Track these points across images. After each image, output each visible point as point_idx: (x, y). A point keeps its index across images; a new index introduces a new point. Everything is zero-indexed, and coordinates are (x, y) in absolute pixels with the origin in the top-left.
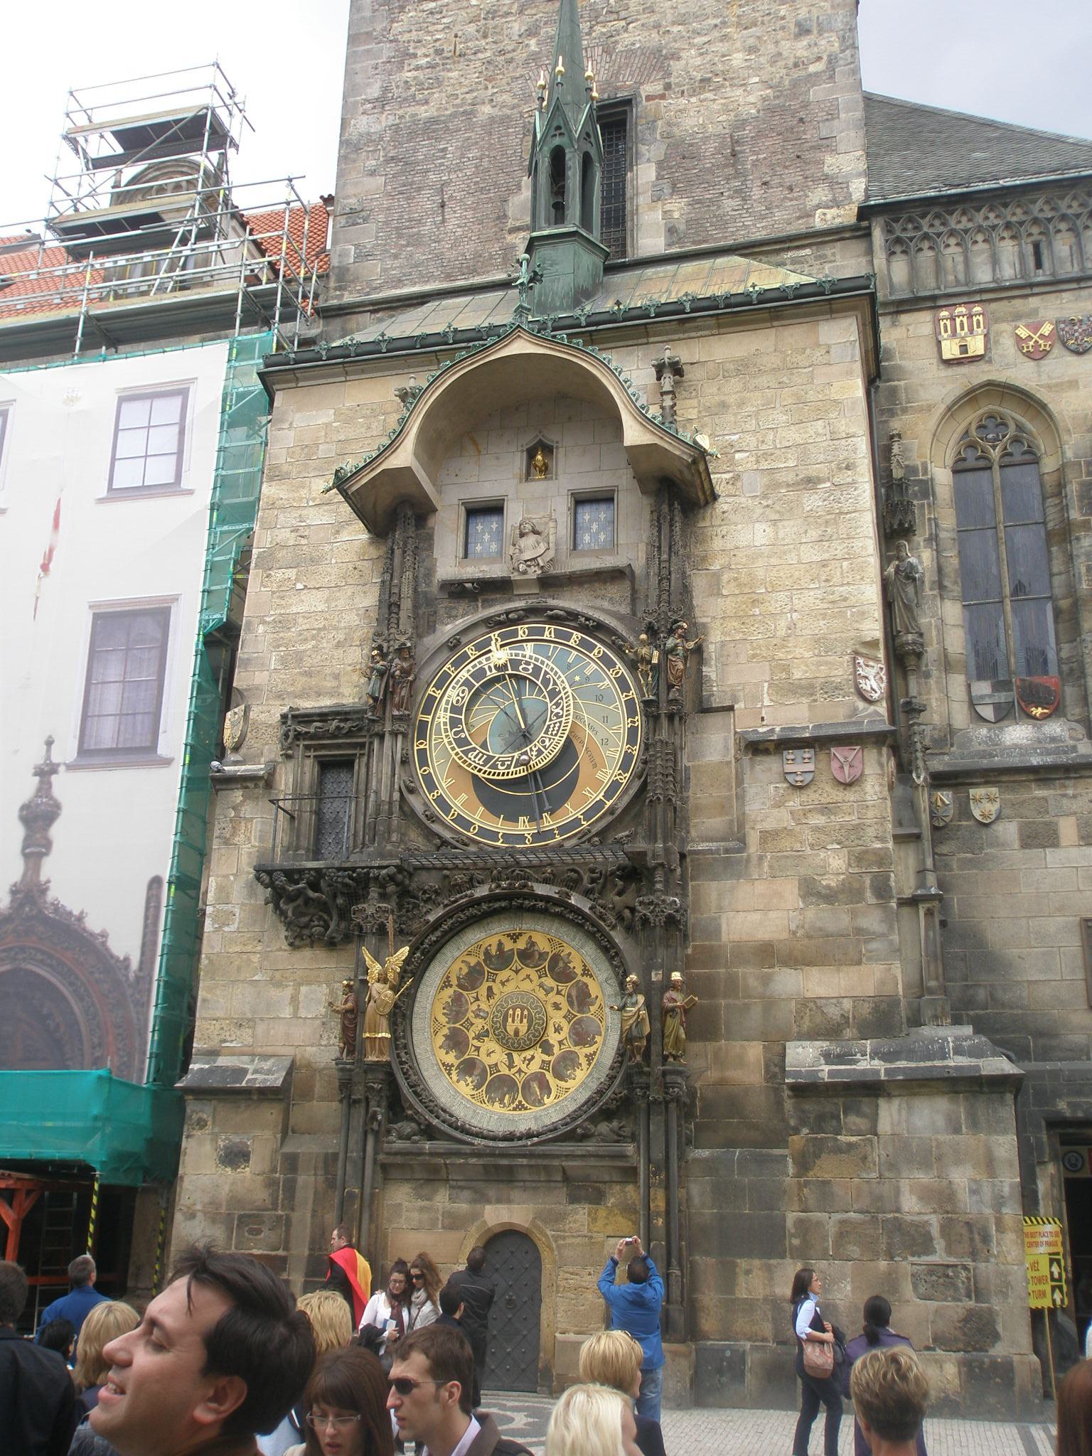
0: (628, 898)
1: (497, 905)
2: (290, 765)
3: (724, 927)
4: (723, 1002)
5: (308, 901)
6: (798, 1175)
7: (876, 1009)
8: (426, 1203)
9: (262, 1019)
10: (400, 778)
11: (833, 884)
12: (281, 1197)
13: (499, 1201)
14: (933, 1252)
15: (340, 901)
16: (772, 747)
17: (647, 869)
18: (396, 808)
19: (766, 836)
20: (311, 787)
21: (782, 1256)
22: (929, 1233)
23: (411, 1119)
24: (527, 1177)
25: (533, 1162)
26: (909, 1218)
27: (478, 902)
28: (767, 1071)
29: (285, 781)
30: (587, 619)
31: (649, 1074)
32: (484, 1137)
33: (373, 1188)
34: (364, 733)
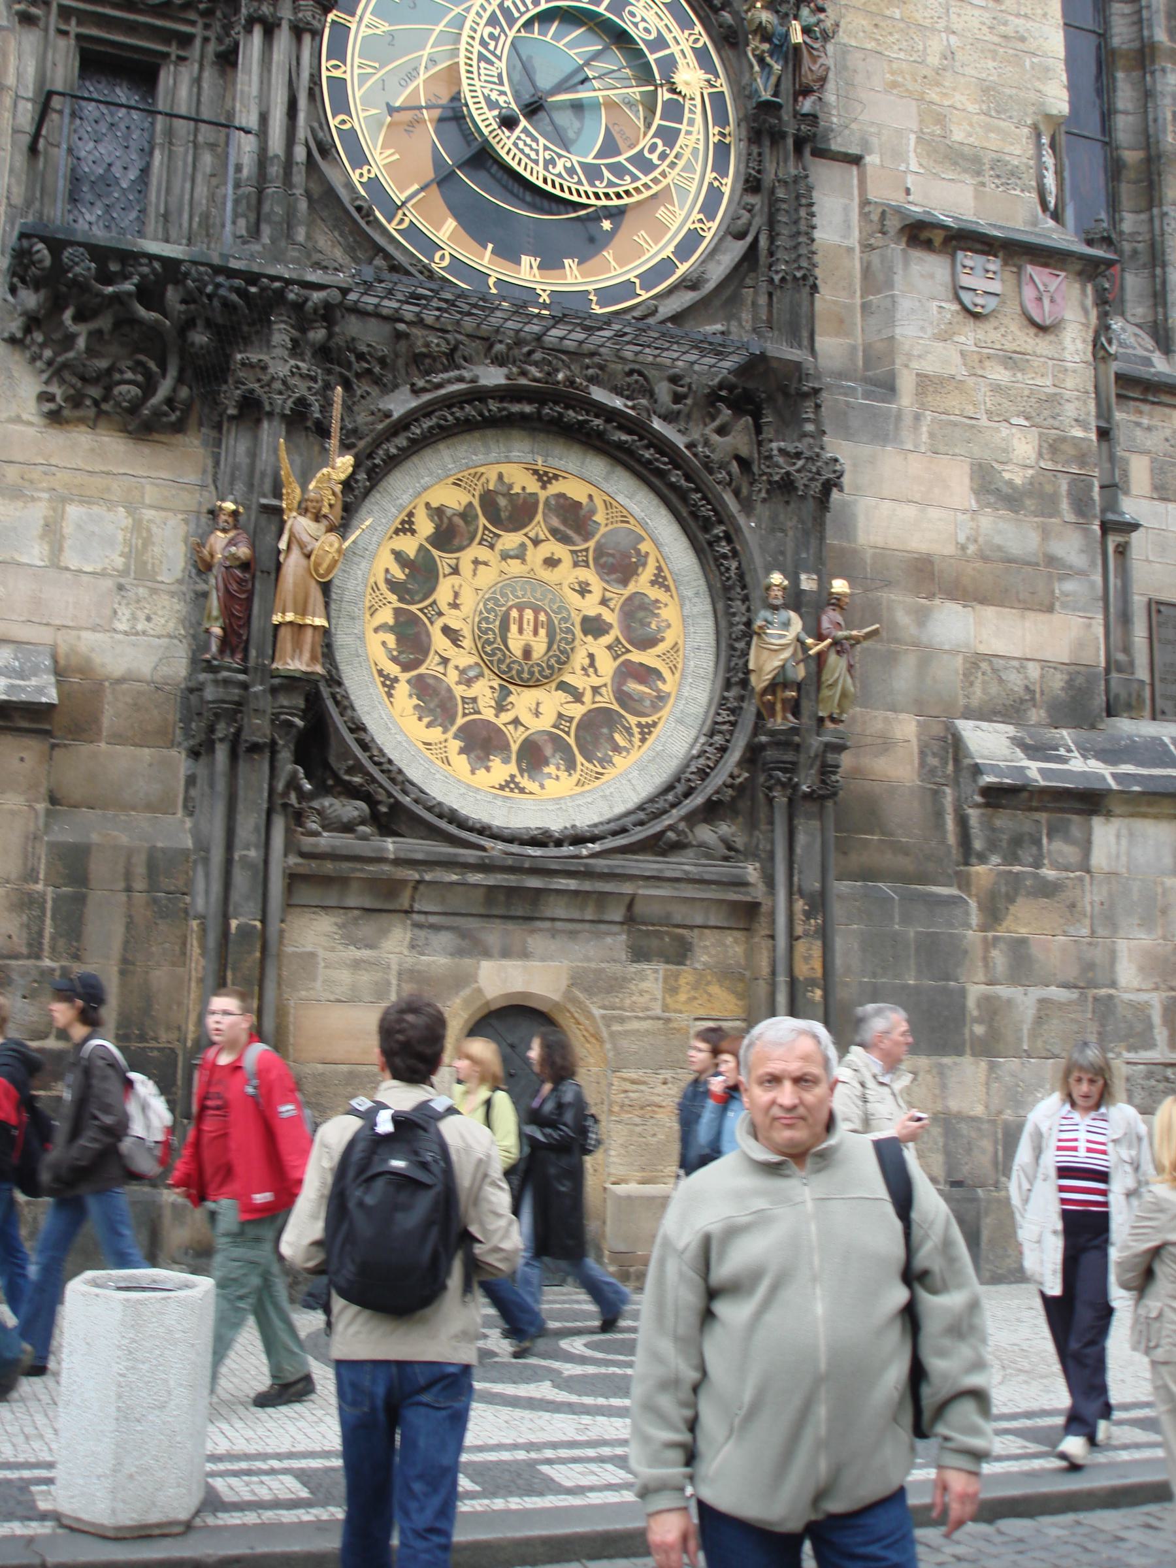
0: (739, 440)
1: (516, 408)
2: (30, 39)
5: (126, 322)
6: (984, 928)
7: (1070, 684)
8: (366, 953)
11: (1018, 481)
12: (49, 930)
13: (506, 954)
14: (1150, 1045)
15: (200, 338)
16: (938, 237)
17: (786, 395)
18: (299, 177)
19: (926, 383)
21: (959, 1052)
22: (1149, 1017)
23: (354, 792)
24: (560, 912)
25: (587, 886)
26: (1127, 996)
27: (479, 395)
28: (923, 763)
31: (797, 748)
32: (495, 836)
34: (192, 16)
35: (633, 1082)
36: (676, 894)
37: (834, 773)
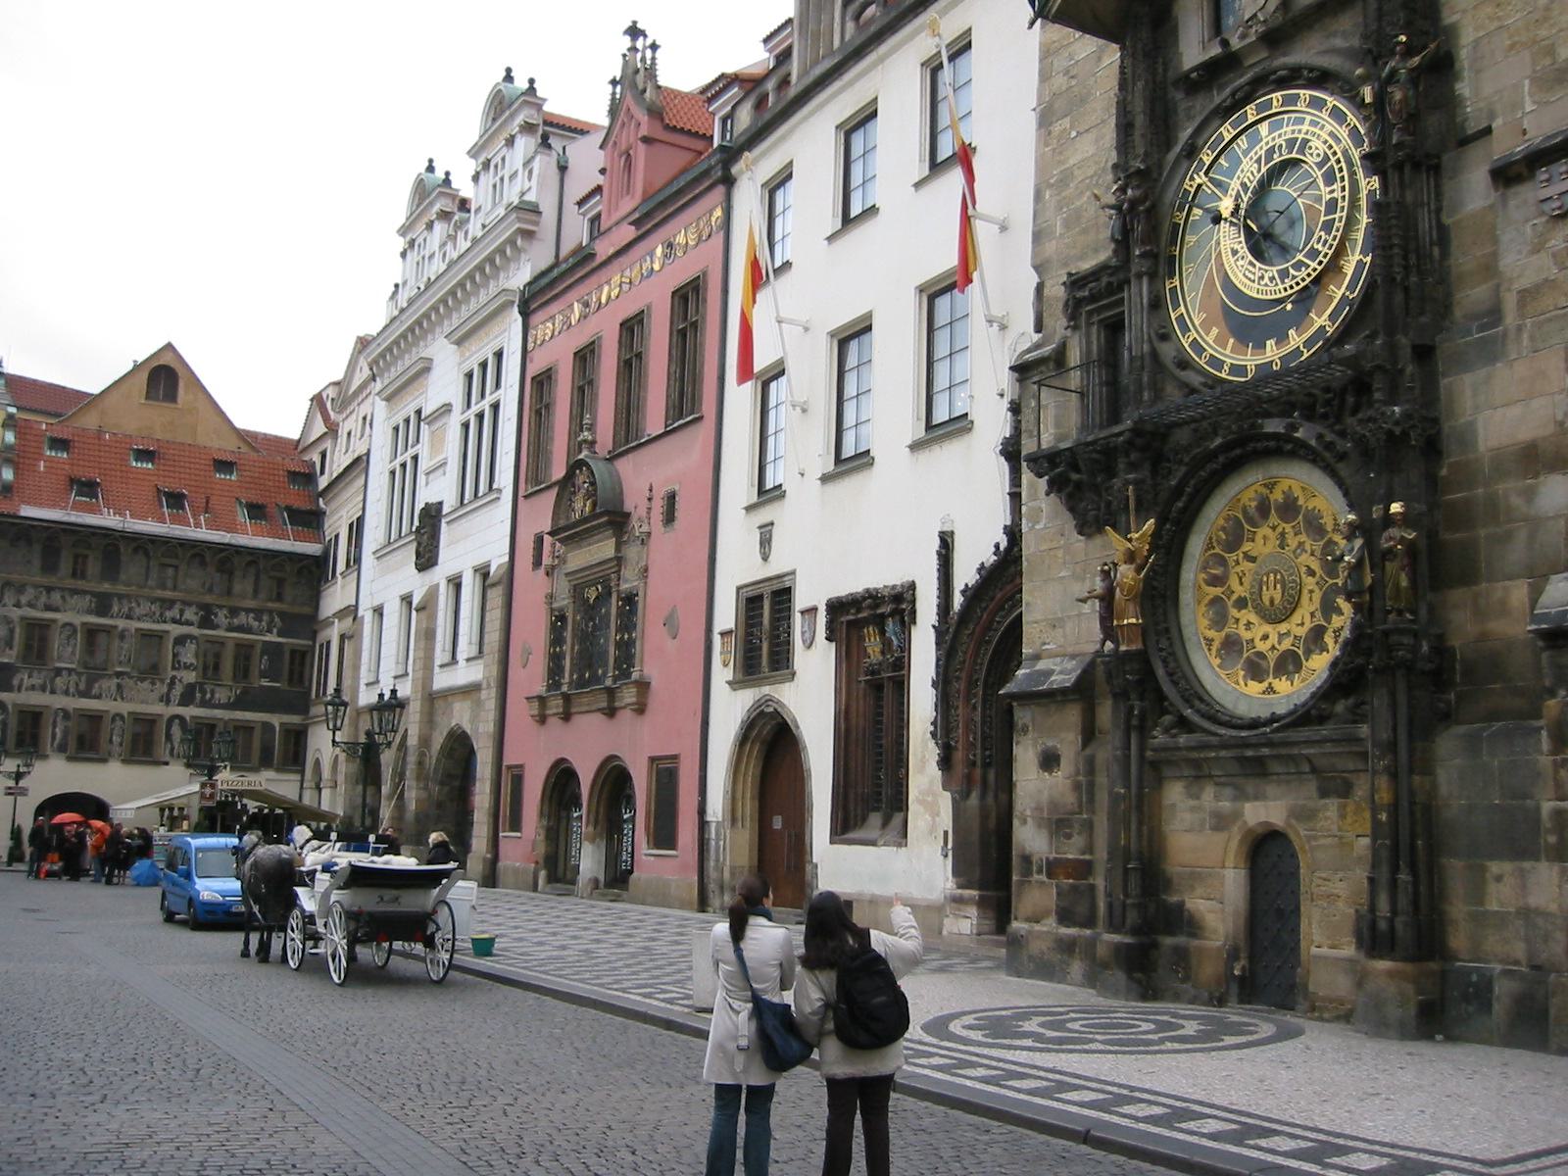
3: (1481, 432)
4: (1482, 533)
6: (1554, 752)
9: (1069, 617)
10: (1149, 327)
12: (1084, 799)
13: (1256, 798)
15: (1099, 479)
20: (1099, 355)
21: (1537, 859)
25: (1275, 752)
27: (1213, 455)
29: (1074, 357)
30: (1311, 70)
31: (1371, 636)
33: (1140, 787)
35: (1325, 880)
36: (1322, 751)
37: (1398, 650)
